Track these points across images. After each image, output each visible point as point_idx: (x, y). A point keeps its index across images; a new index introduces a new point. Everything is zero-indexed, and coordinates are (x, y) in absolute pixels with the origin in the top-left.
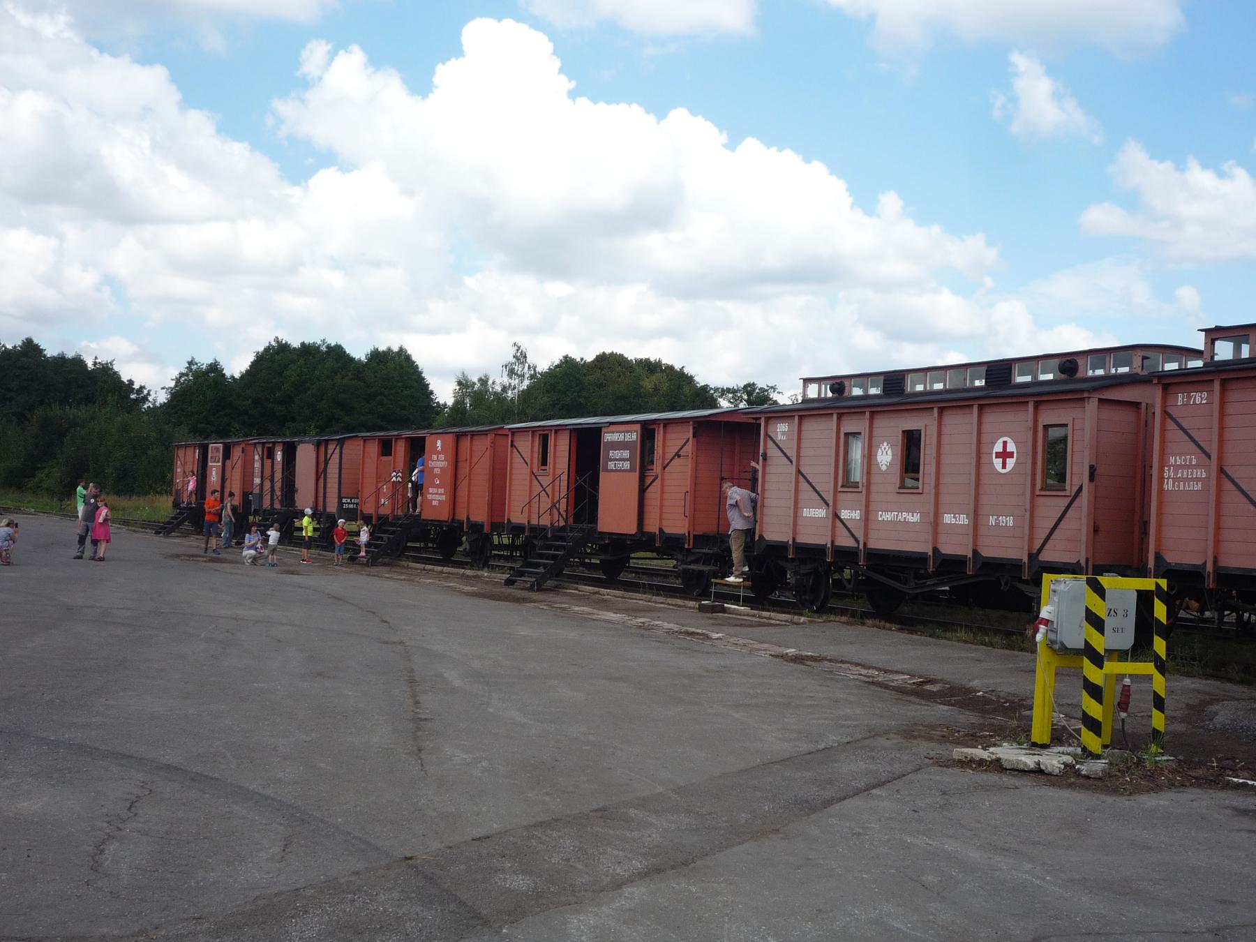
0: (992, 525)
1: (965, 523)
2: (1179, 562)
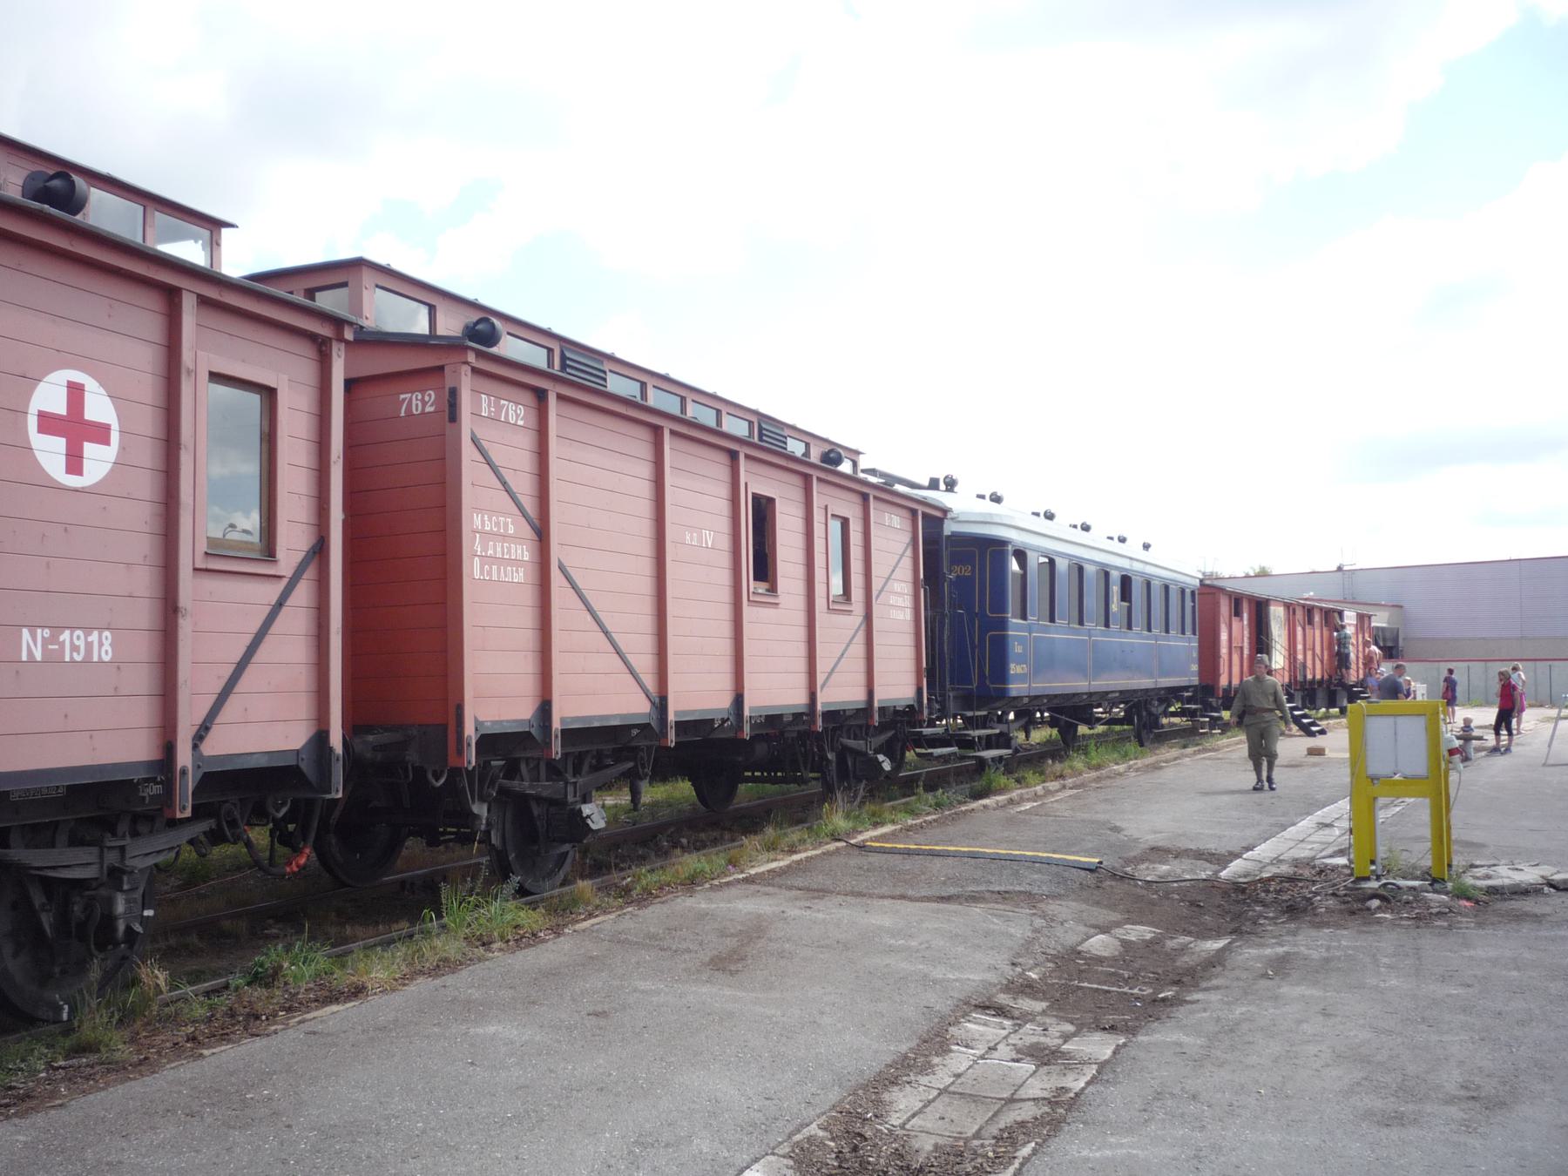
0: (31, 660)
2: (497, 719)
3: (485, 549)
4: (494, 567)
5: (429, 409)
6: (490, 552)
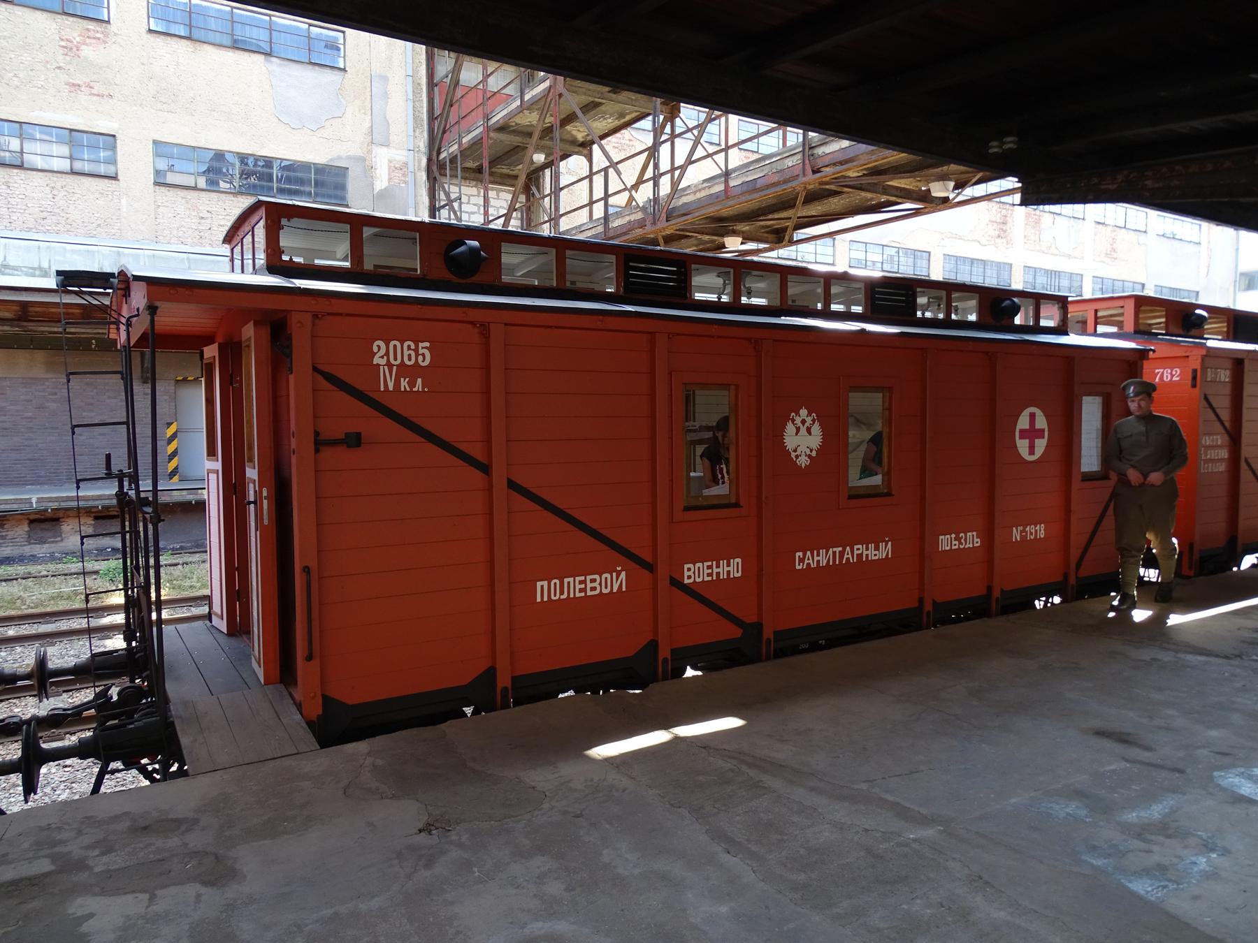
1: (976, 545)
3: (1206, 455)
4: (1210, 465)
5: (1175, 379)
6: (1209, 457)
